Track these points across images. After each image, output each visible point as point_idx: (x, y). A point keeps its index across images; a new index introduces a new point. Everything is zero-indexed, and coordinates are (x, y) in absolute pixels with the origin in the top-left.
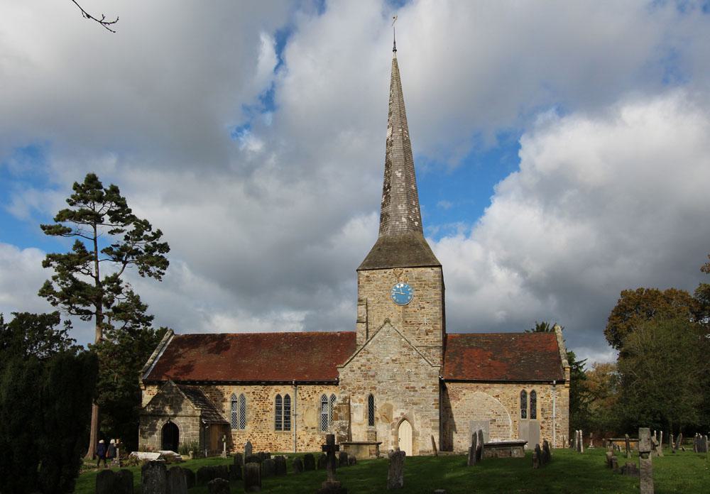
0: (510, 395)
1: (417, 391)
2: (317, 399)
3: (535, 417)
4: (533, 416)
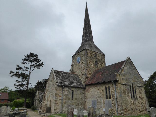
4: (110, 98)
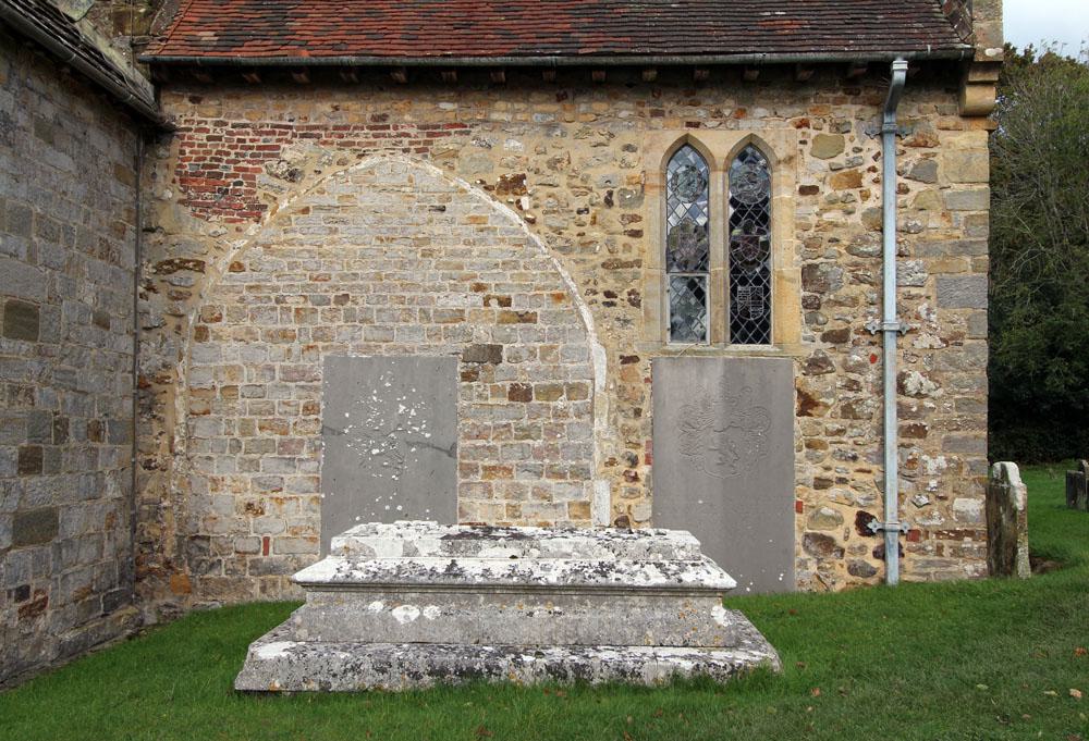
0: (597, 174)
4: (751, 325)
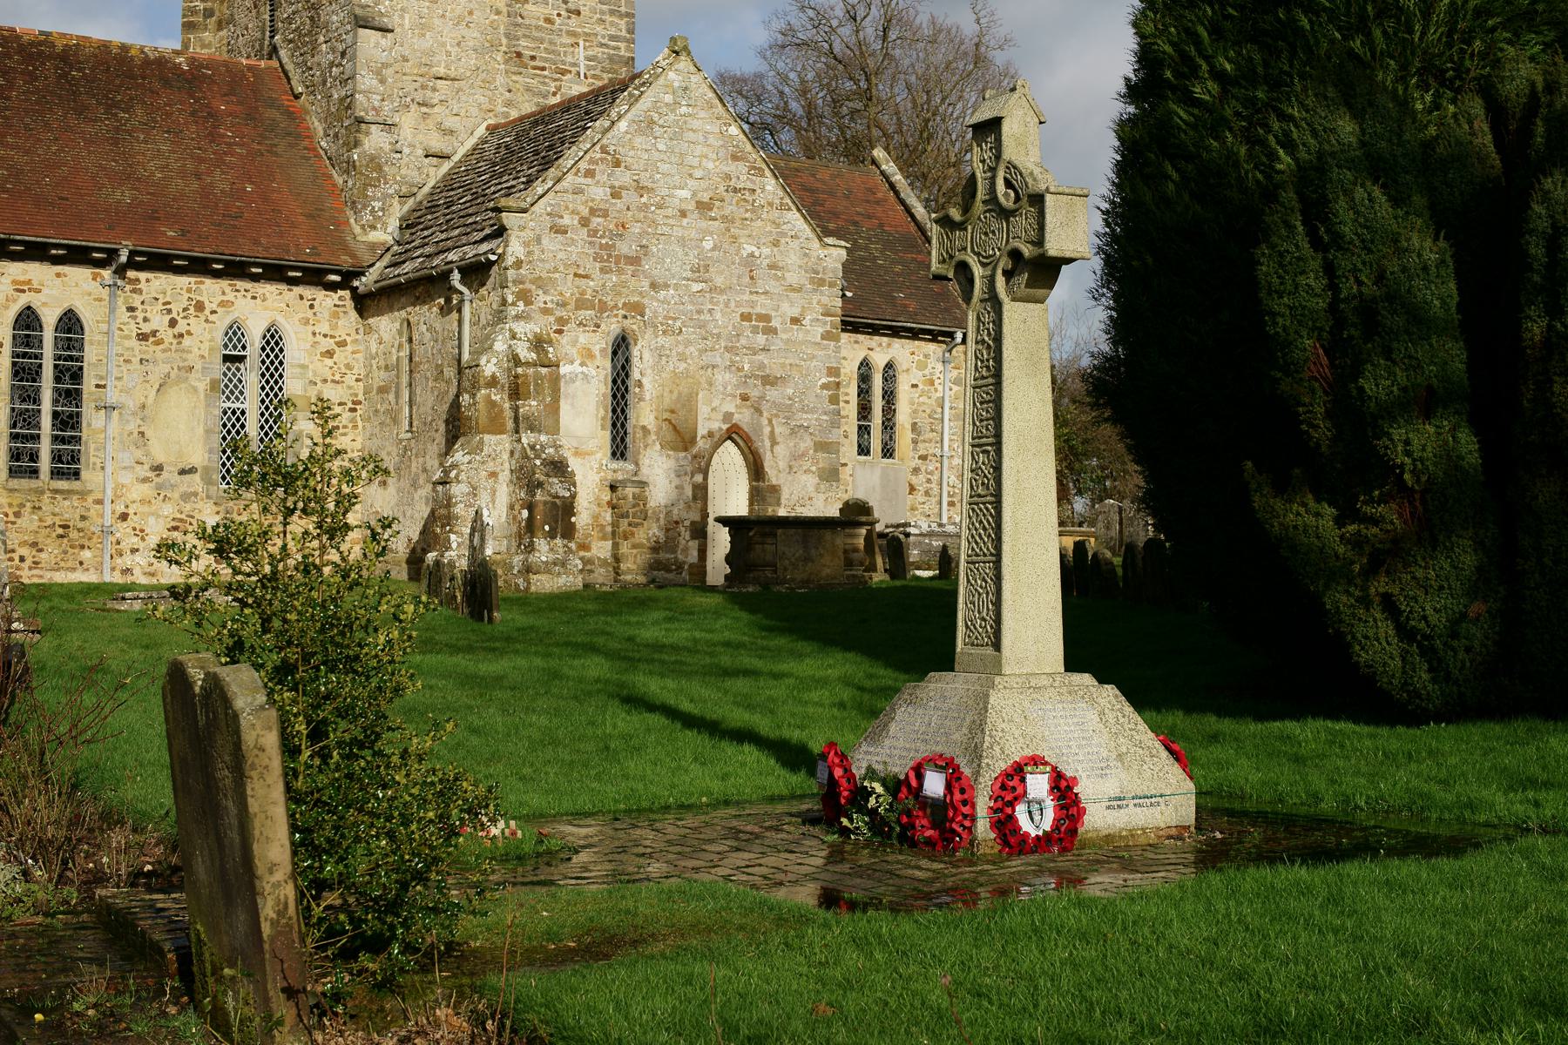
1: (774, 331)
2: (205, 339)
3: (868, 453)
4: (888, 452)
